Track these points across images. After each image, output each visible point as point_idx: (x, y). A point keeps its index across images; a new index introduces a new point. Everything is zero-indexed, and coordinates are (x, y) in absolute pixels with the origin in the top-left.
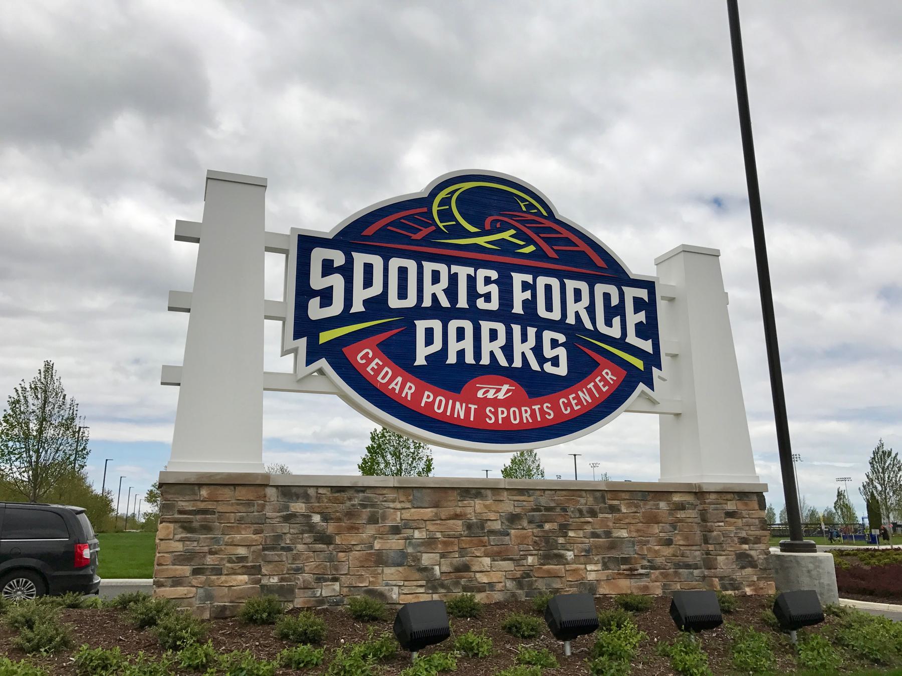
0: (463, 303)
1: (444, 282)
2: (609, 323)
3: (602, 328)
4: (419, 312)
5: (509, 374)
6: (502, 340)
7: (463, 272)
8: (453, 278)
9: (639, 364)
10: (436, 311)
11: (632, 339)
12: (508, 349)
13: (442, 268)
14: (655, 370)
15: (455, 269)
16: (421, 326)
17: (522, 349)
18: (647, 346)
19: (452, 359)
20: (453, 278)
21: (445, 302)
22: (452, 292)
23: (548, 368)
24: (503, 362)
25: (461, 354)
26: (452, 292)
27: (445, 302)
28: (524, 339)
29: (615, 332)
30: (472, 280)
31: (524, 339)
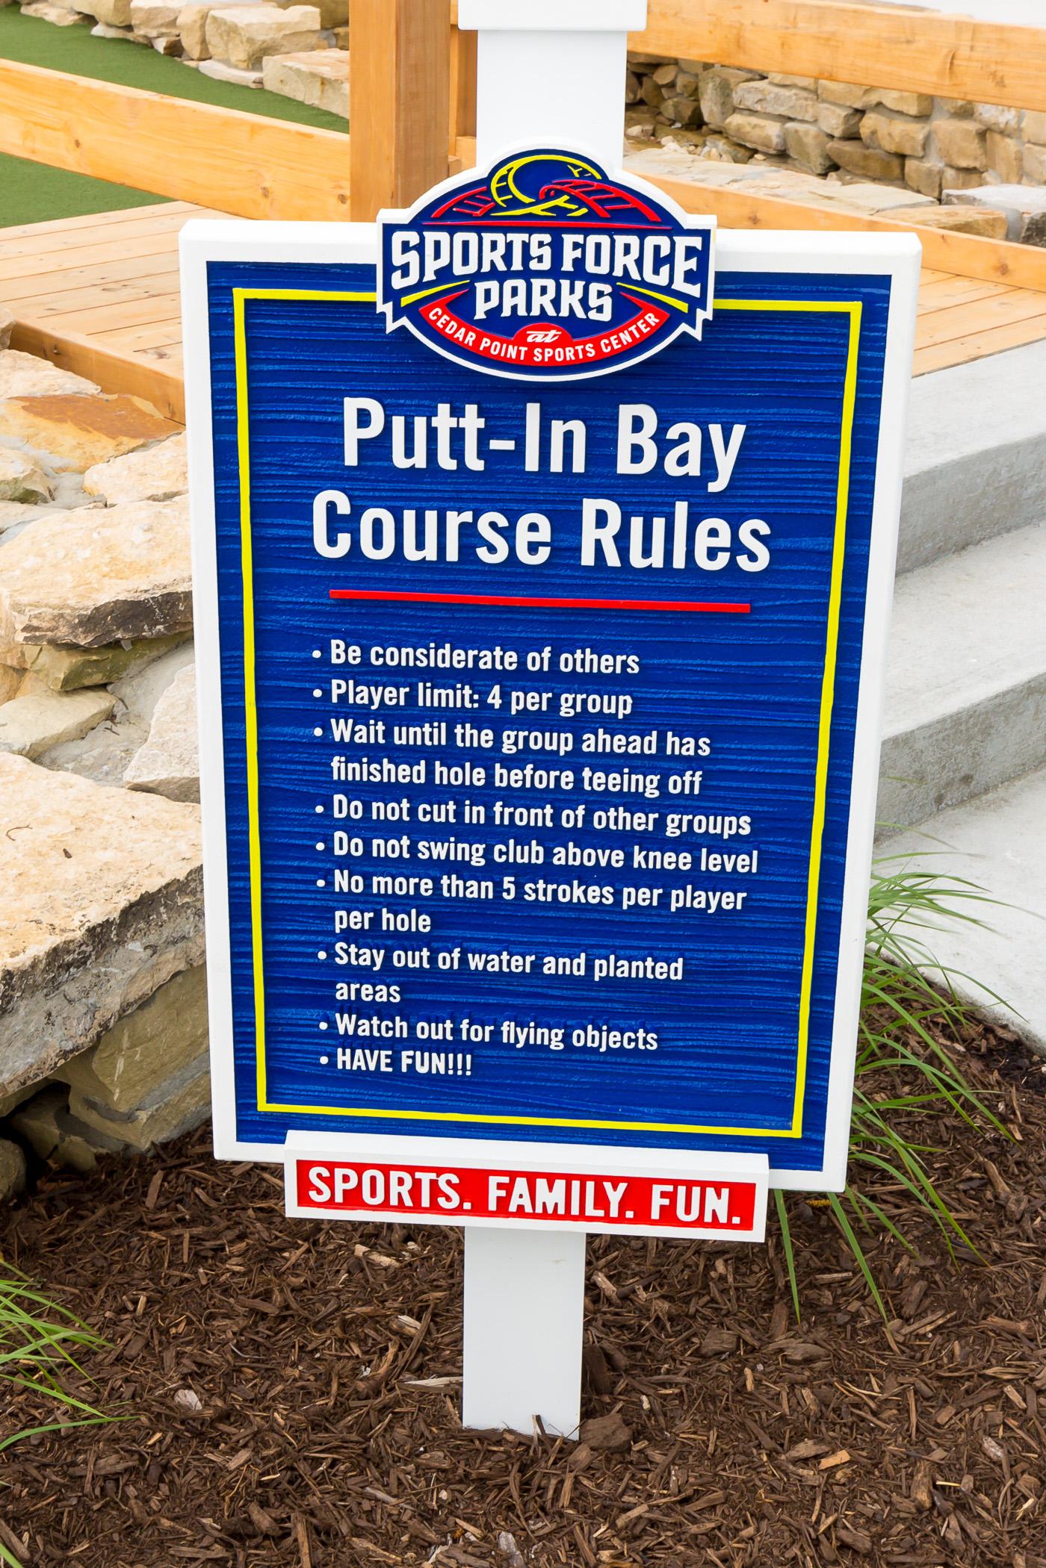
0: (517, 265)
1: (501, 249)
2: (656, 272)
3: (649, 277)
4: (479, 276)
5: (558, 321)
6: (551, 293)
7: (518, 239)
8: (509, 246)
9: (683, 307)
10: (494, 274)
11: (679, 285)
12: (556, 302)
13: (499, 237)
14: (699, 311)
15: (511, 236)
16: (481, 287)
17: (570, 301)
18: (694, 290)
19: (506, 312)
20: (509, 246)
21: (501, 267)
22: (507, 258)
23: (593, 315)
24: (551, 311)
25: (514, 308)
26: (507, 258)
27: (501, 267)
28: (572, 291)
29: (662, 280)
30: (526, 246)
31: (572, 291)
